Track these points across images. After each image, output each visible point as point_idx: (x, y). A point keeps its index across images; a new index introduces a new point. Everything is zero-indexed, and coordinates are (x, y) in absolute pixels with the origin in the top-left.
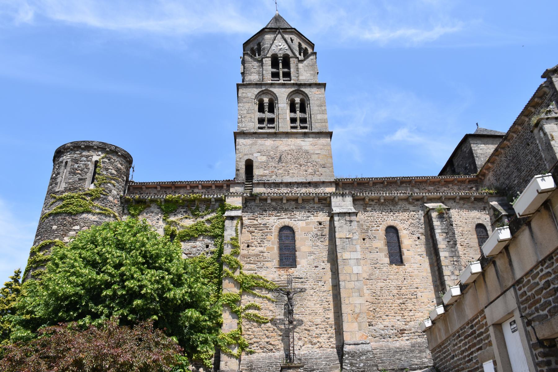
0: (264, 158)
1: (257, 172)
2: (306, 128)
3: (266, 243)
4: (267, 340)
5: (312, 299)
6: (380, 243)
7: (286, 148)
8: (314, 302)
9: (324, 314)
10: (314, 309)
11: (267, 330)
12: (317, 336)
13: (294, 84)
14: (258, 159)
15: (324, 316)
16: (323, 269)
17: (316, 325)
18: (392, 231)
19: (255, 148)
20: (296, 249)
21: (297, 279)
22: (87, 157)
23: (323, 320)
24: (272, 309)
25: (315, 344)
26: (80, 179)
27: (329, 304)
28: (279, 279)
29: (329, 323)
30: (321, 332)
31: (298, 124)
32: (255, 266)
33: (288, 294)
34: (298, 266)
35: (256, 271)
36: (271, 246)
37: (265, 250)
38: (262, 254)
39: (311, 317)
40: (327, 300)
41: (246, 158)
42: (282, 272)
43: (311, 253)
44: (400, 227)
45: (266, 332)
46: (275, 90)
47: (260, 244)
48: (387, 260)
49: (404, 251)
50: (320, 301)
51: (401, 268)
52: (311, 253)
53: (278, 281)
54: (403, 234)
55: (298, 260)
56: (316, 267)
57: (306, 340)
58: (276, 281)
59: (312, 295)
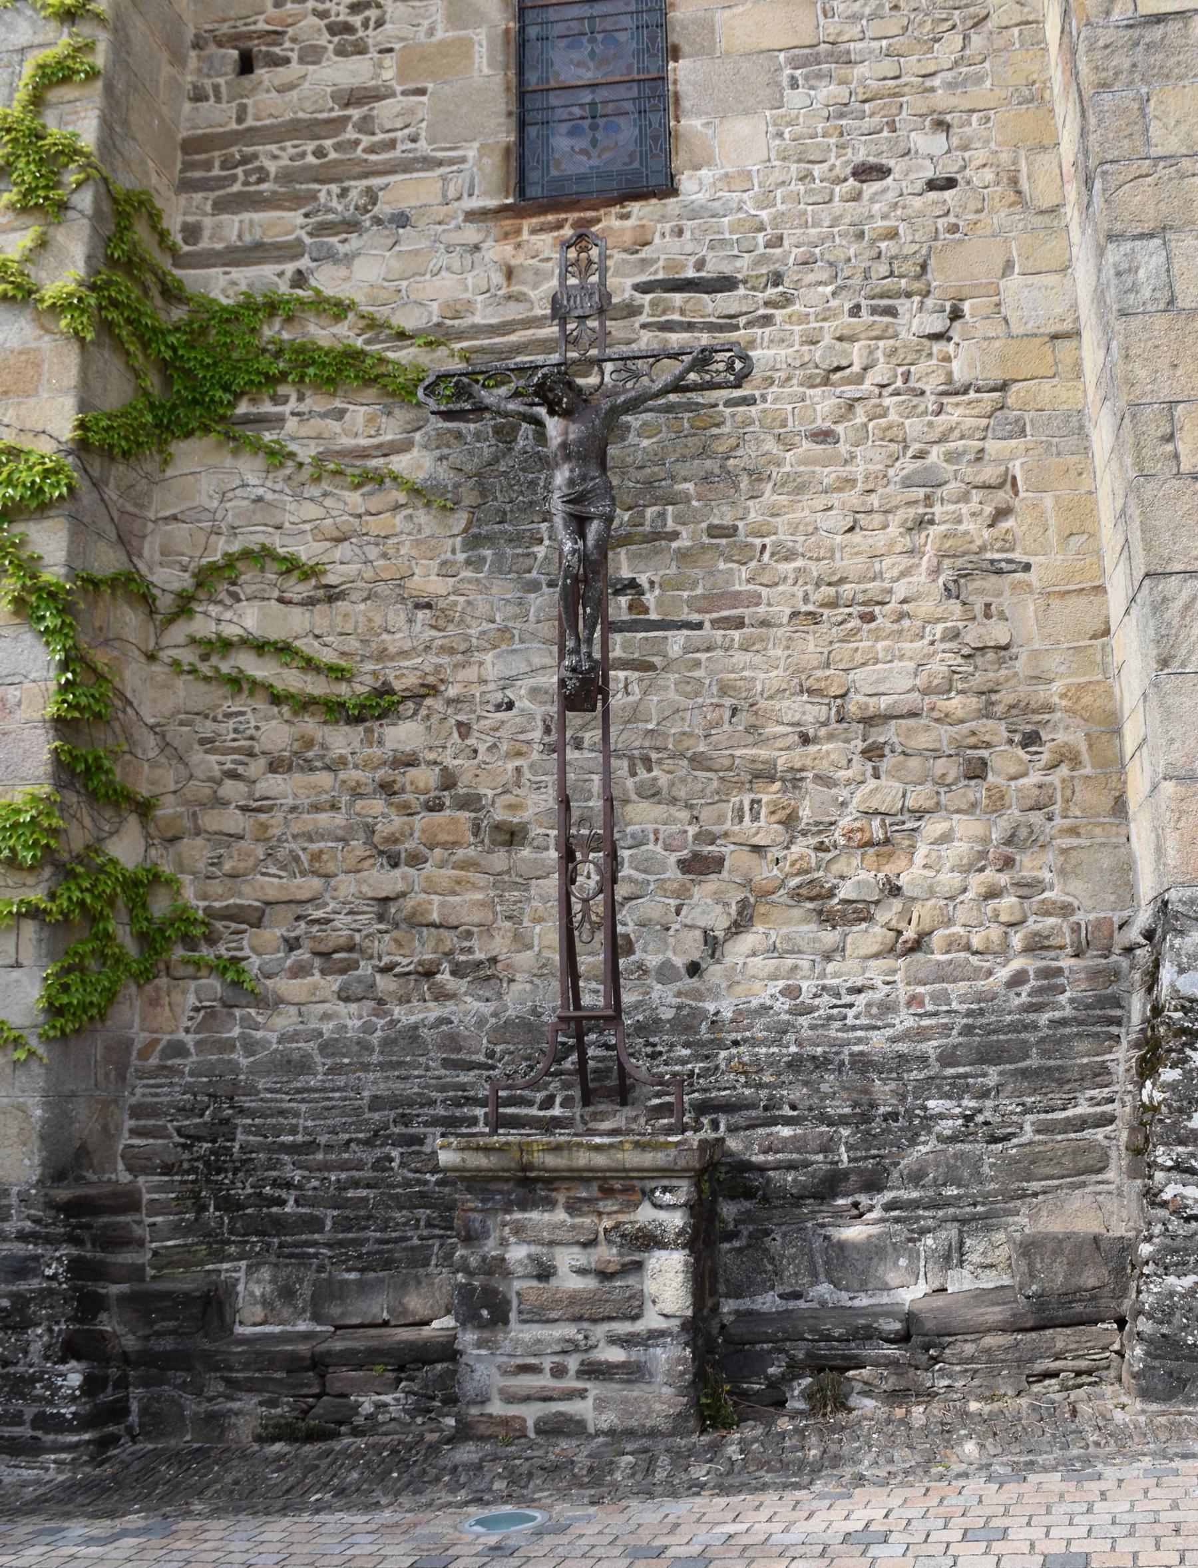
4: (387, 881)
5: (828, 474)
8: (852, 497)
9: (955, 607)
10: (845, 564)
11: (387, 789)
12: (876, 829)
15: (954, 635)
16: (932, 185)
17: (869, 721)
20: (674, 38)
21: (678, 298)
23: (938, 667)
24: (436, 586)
25: (859, 913)
27: (1002, 513)
28: (514, 312)
29: (1006, 697)
30: (918, 797)
32: (297, 217)
34: (687, 183)
35: (304, 263)
36: (440, 35)
37: (388, 74)
38: (356, 113)
39: (811, 646)
40: (989, 473)
45: (377, 805)
47: (348, 28)
50: (907, 483)
53: (493, 330)
55: (691, 124)
56: (868, 172)
57: (766, 872)
58: (478, 331)
59: (824, 436)
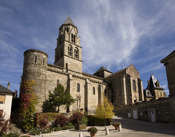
0: (70, 64)
1: (69, 67)
2: (77, 58)
3: (75, 86)
6: (92, 90)
7: (74, 63)
13: (76, 45)
14: (69, 64)
18: (94, 88)
19: (68, 60)
22: (42, 56)
26: (41, 62)
31: (76, 56)
33: (80, 97)
41: (66, 62)
42: (78, 93)
43: (82, 90)
44: (95, 87)
46: (73, 45)
48: (93, 93)
49: (95, 92)
51: (95, 95)
52: (82, 90)
54: (95, 89)
